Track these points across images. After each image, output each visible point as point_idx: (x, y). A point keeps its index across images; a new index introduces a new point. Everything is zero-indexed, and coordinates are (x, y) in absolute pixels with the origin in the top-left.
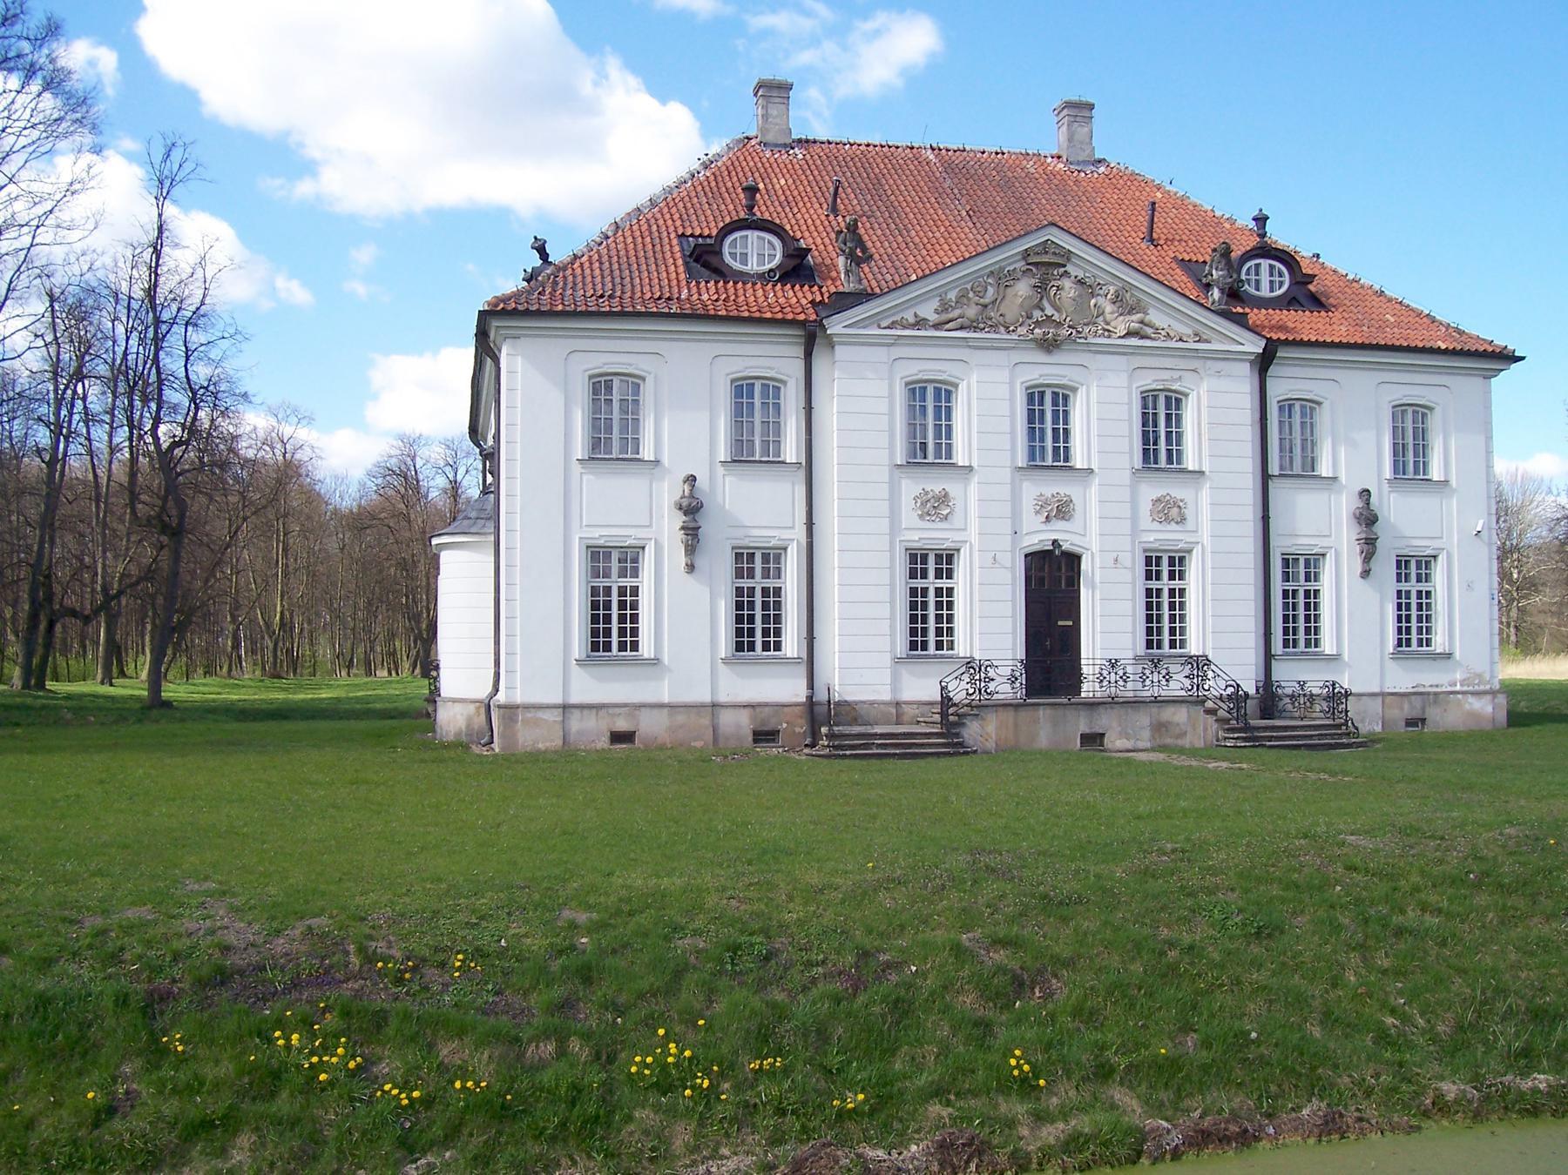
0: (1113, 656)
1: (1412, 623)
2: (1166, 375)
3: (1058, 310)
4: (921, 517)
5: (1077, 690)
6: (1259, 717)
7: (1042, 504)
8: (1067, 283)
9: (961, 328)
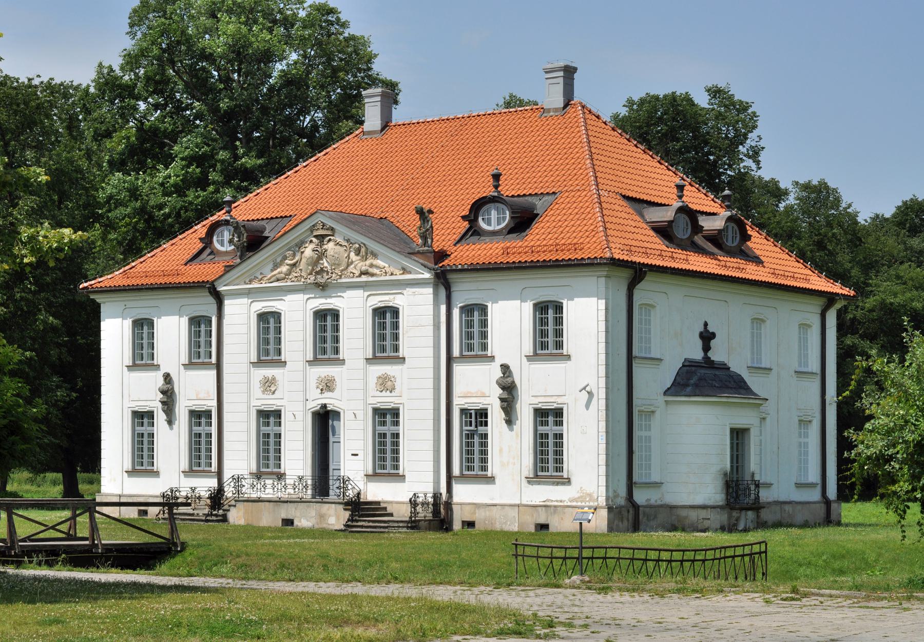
1: (548, 459)
2: (386, 298)
4: (263, 392)
7: (320, 380)
8: (331, 245)
9: (278, 280)
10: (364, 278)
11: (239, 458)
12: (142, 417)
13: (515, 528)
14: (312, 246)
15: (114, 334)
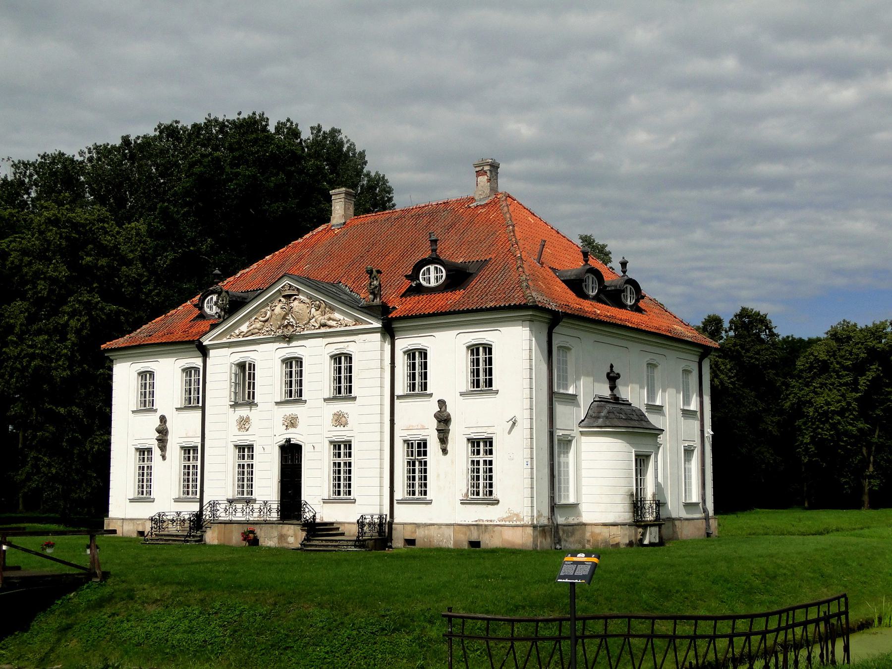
6: (379, 535)
7: (285, 418)
8: (296, 303)
10: (323, 330)
11: (220, 485)
12: (144, 452)
13: (451, 545)
14: (281, 305)
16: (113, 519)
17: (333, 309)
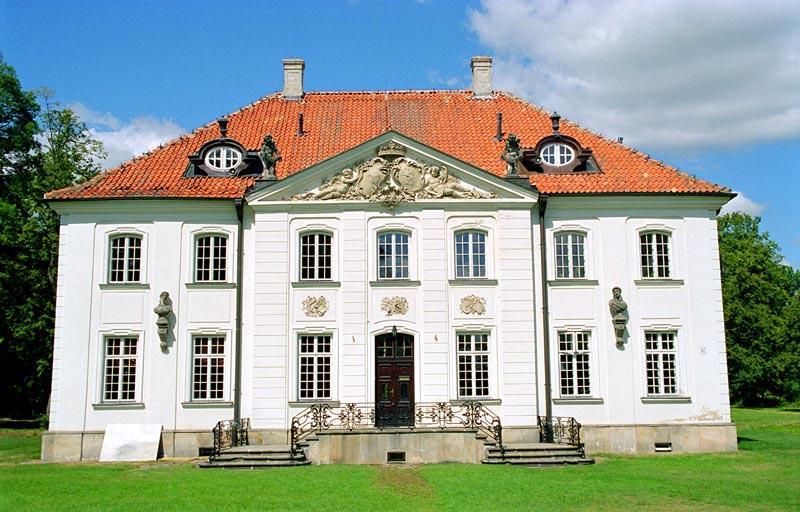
0: (351, 401)
1: (661, 377)
3: (399, 183)
5: (410, 421)
8: (403, 166)
9: (333, 198)
12: (120, 345)
13: (633, 450)
15: (81, 248)
16: (53, 433)
17: (457, 176)
